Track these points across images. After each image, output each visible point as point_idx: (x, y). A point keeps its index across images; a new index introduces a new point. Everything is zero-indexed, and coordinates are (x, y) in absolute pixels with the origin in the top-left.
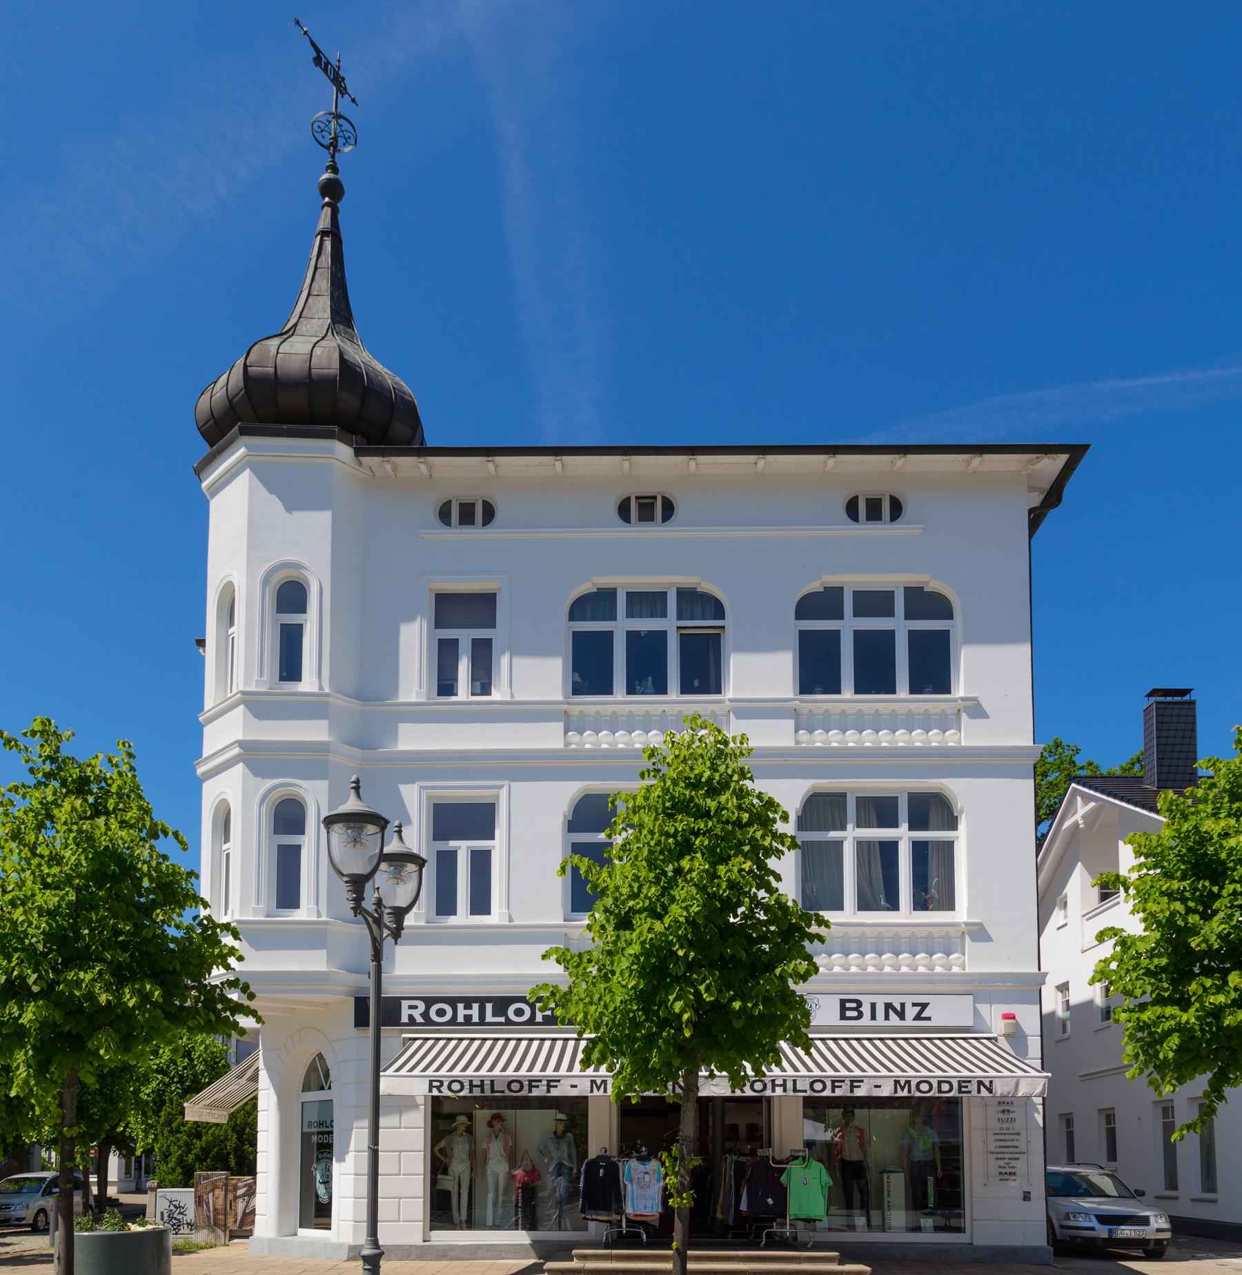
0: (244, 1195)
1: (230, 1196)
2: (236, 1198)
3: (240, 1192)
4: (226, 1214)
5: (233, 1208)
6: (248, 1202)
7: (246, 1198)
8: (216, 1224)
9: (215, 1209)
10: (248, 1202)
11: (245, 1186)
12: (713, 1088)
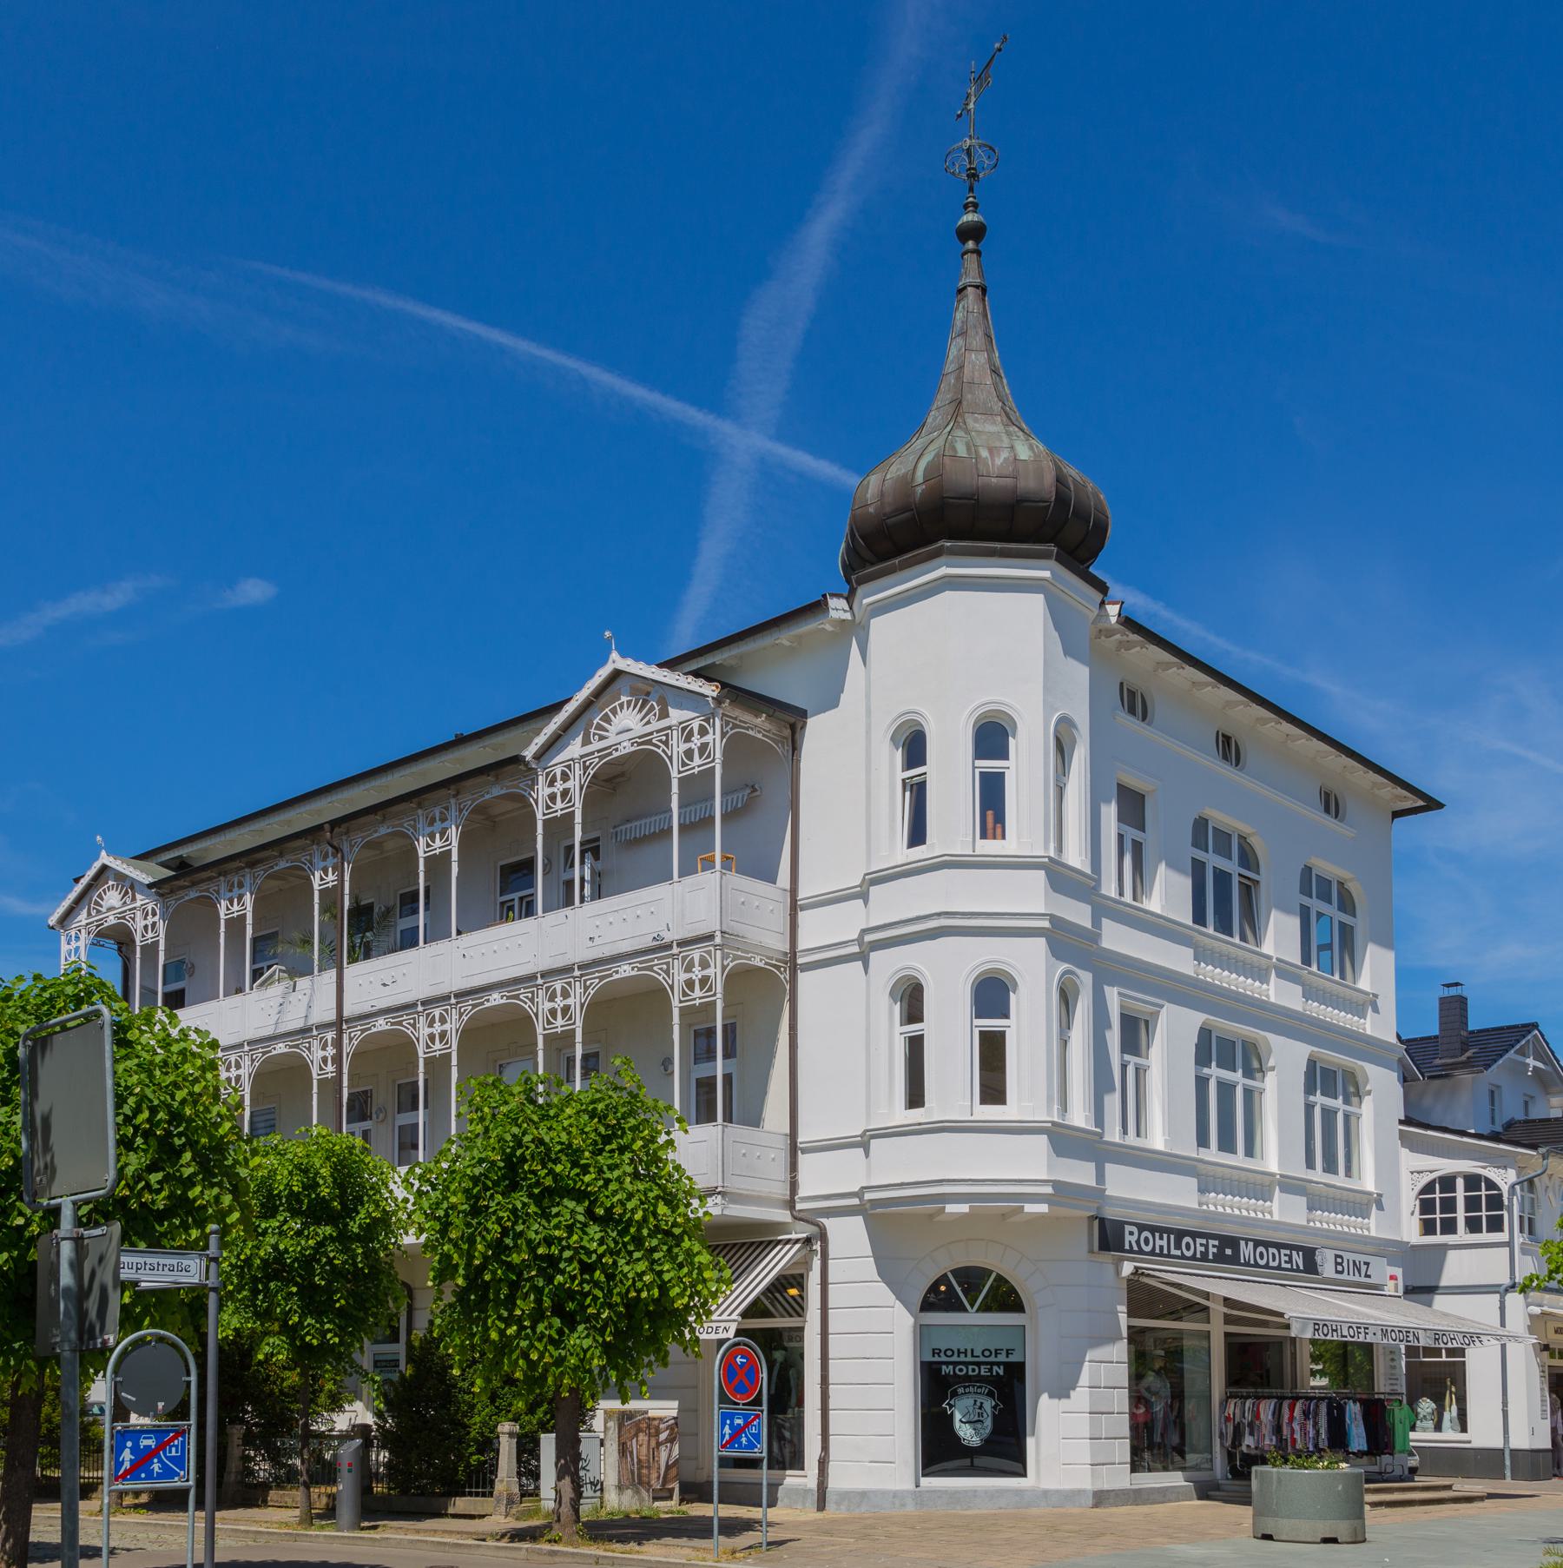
0: (667, 1441)
1: (653, 1444)
2: (659, 1444)
3: (663, 1436)
4: (649, 1468)
5: (656, 1459)
6: (671, 1450)
7: (669, 1445)
8: (640, 1482)
9: (639, 1461)
10: (671, 1450)
11: (667, 1429)
12: (1492, 1174)
